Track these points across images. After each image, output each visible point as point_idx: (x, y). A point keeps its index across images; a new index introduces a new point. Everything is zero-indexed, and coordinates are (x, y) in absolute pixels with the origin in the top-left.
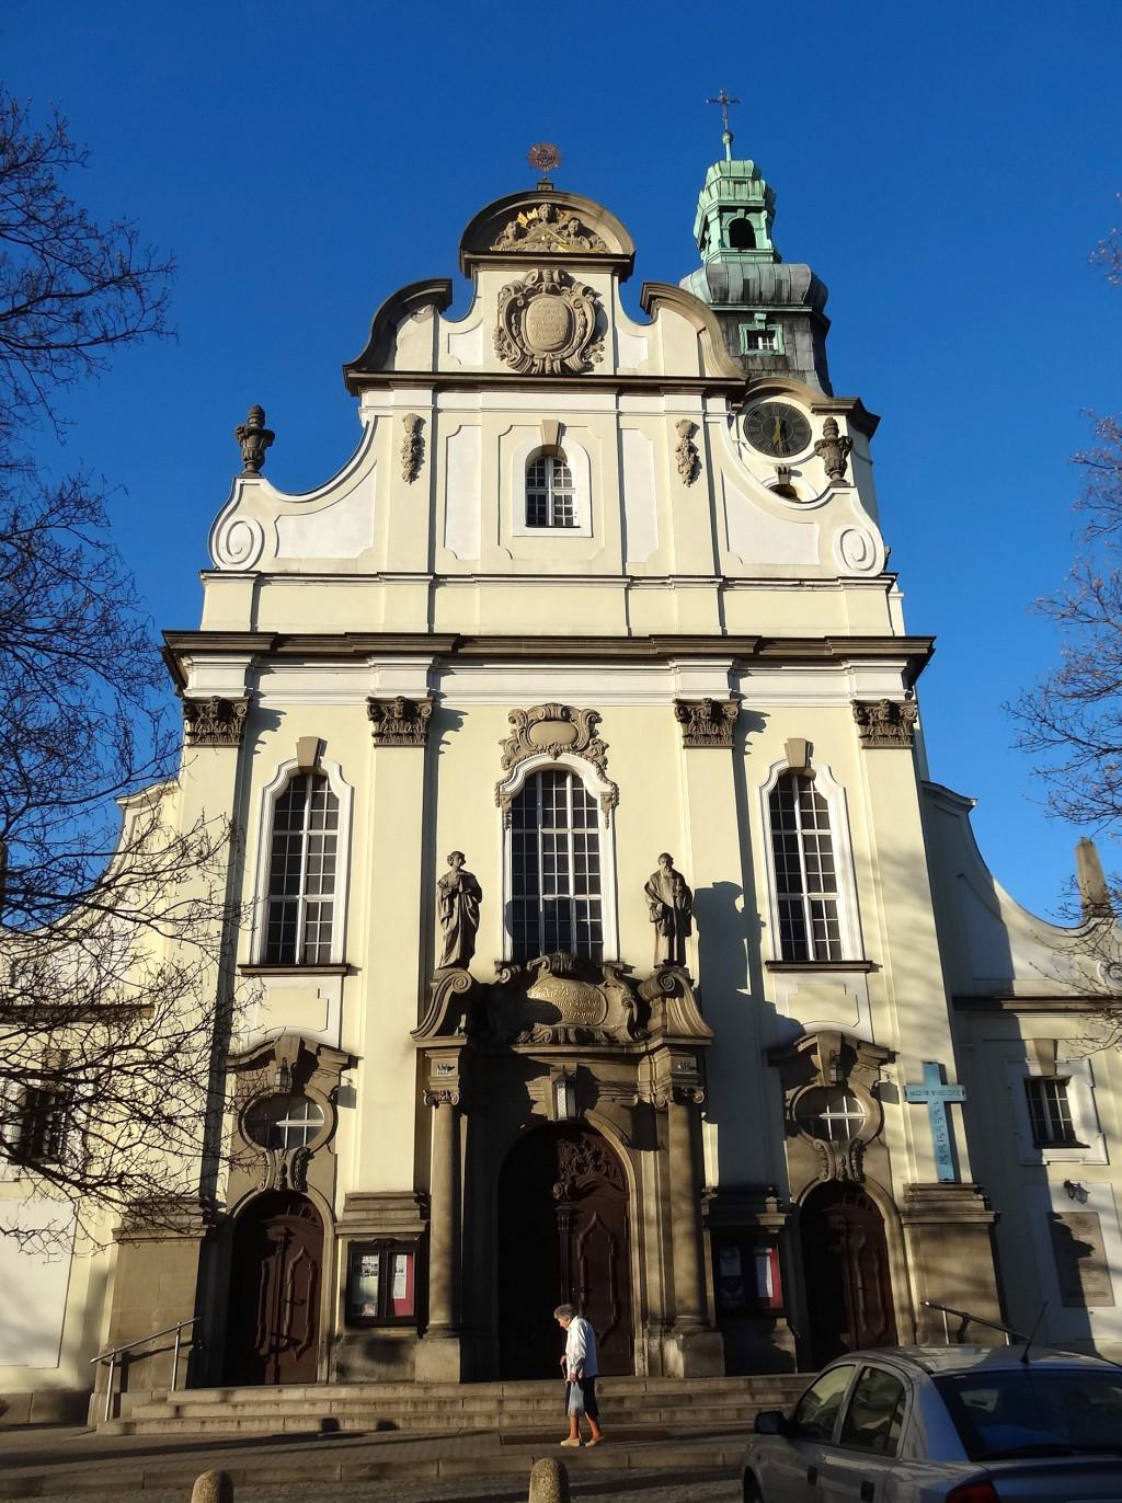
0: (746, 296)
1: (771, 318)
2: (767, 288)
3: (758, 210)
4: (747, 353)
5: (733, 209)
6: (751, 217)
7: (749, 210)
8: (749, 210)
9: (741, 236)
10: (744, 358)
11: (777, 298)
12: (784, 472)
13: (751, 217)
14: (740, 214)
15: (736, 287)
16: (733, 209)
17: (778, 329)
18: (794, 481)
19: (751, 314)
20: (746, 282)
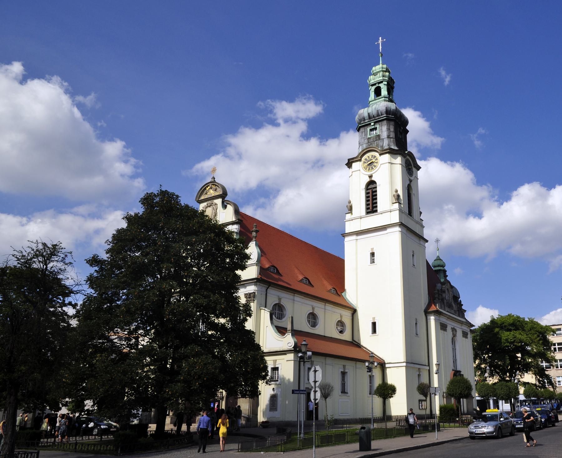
0: (370, 117)
1: (375, 123)
2: (375, 113)
3: (382, 82)
4: (369, 137)
5: (375, 84)
6: (381, 85)
7: (379, 83)
8: (379, 83)
9: (378, 92)
10: (369, 138)
11: (378, 115)
12: (371, 177)
13: (381, 85)
14: (377, 85)
15: (366, 115)
16: (375, 84)
17: (377, 126)
18: (373, 179)
19: (370, 124)
20: (369, 114)
